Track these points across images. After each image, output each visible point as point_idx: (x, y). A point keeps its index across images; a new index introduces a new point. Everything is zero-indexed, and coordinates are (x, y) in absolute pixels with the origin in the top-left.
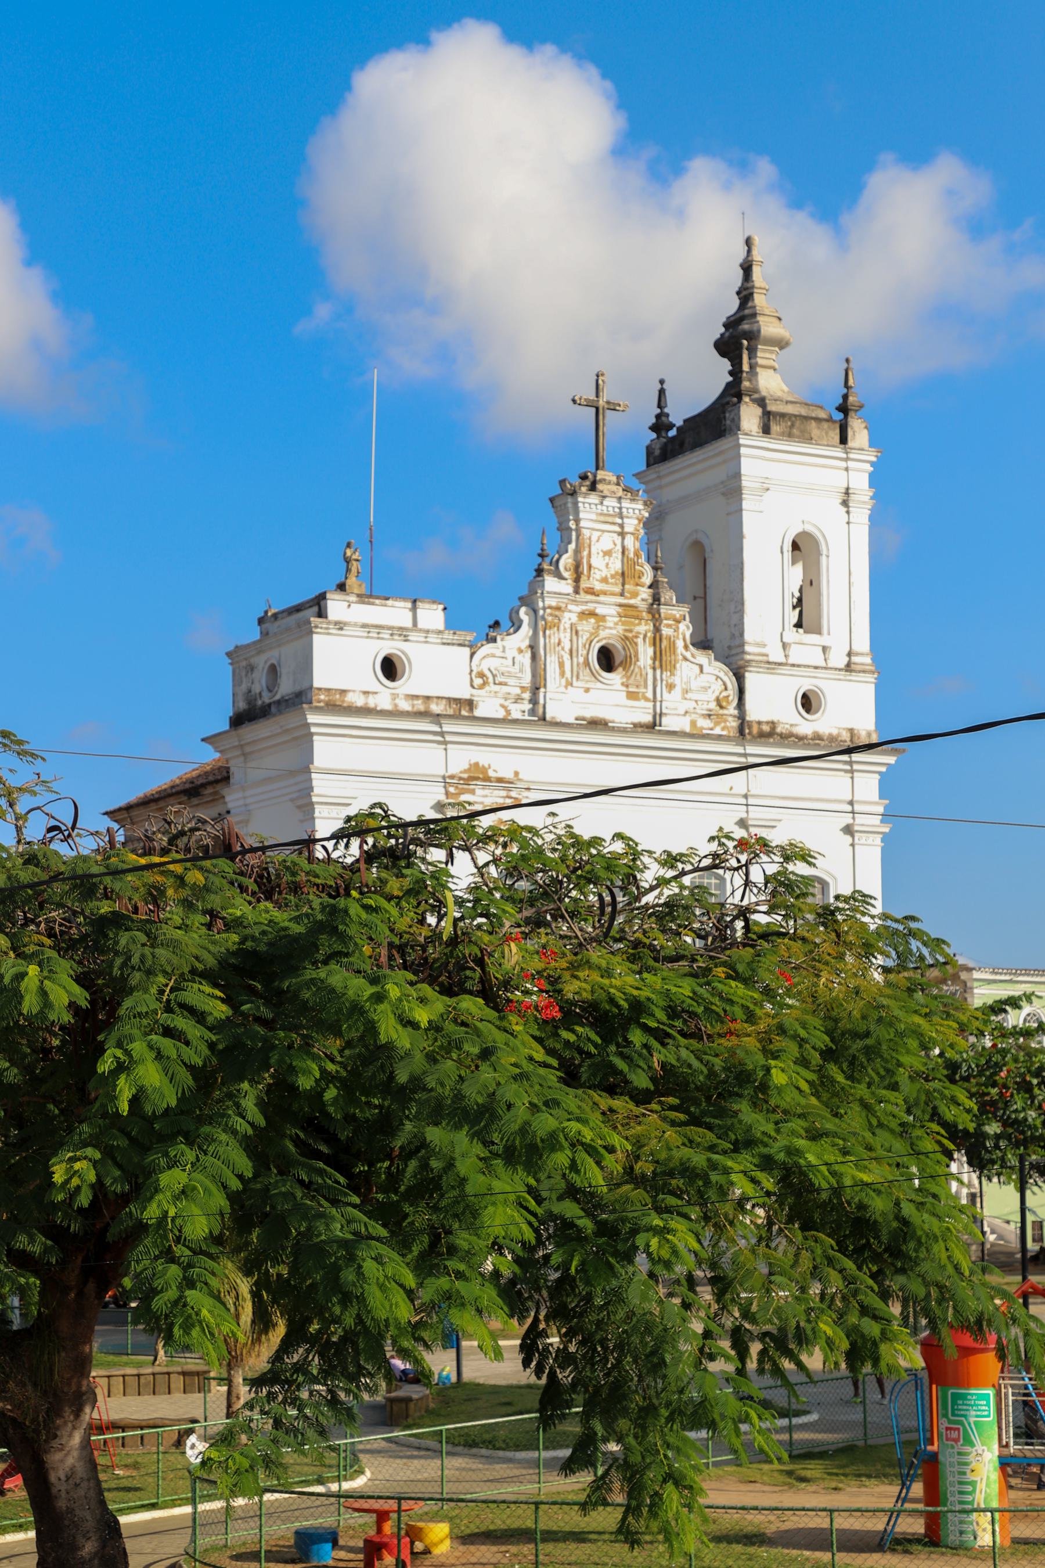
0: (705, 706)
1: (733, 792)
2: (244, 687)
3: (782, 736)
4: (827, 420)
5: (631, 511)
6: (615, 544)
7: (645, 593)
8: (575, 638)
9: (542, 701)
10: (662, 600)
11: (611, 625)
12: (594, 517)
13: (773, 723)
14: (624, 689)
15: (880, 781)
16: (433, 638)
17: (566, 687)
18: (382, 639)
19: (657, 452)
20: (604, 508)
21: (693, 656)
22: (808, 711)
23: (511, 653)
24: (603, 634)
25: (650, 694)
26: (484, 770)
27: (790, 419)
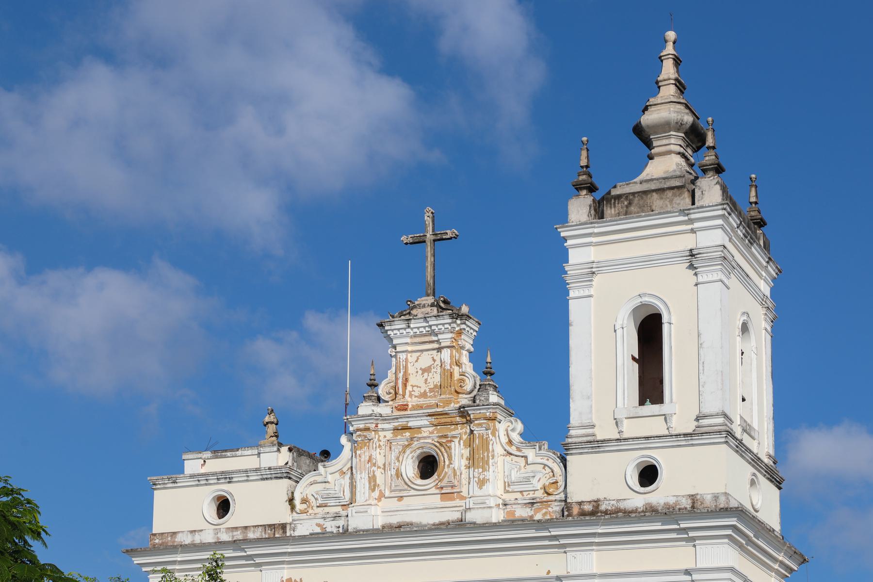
0: (531, 495)
3: (606, 512)
6: (434, 360)
12: (408, 340)
14: (437, 491)
21: (518, 449)
27: (627, 198)
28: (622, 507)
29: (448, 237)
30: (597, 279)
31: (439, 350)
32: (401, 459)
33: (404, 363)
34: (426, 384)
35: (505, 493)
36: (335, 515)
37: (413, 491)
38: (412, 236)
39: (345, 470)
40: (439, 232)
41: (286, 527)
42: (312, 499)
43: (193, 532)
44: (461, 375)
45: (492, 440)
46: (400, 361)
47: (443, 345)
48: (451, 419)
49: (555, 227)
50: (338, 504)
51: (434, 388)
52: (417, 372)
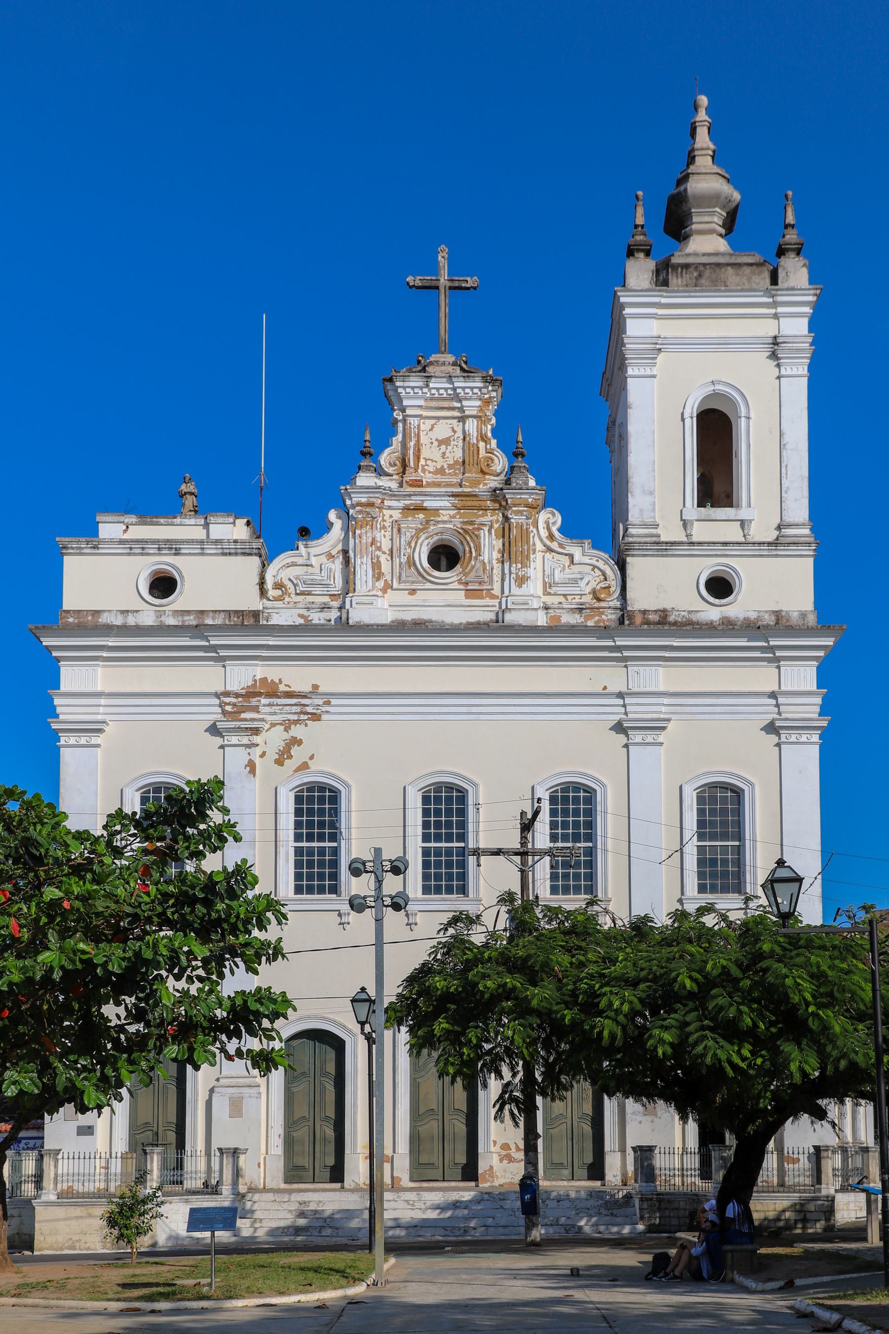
3: (675, 623)
6: (454, 432)
11: (446, 518)
12: (421, 402)
13: (664, 611)
14: (462, 587)
15: (818, 668)
20: (434, 391)
25: (497, 591)
29: (468, 286)
30: (661, 357)
31: (462, 419)
32: (413, 545)
33: (416, 430)
34: (443, 458)
35: (544, 595)
36: (323, 606)
37: (428, 584)
38: (422, 278)
39: (334, 552)
40: (456, 278)
41: (259, 615)
42: (289, 585)
44: (488, 453)
45: (532, 531)
46: (410, 428)
47: (467, 413)
48: (479, 502)
49: (616, 289)
50: (326, 593)
51: (454, 464)
52: (432, 443)
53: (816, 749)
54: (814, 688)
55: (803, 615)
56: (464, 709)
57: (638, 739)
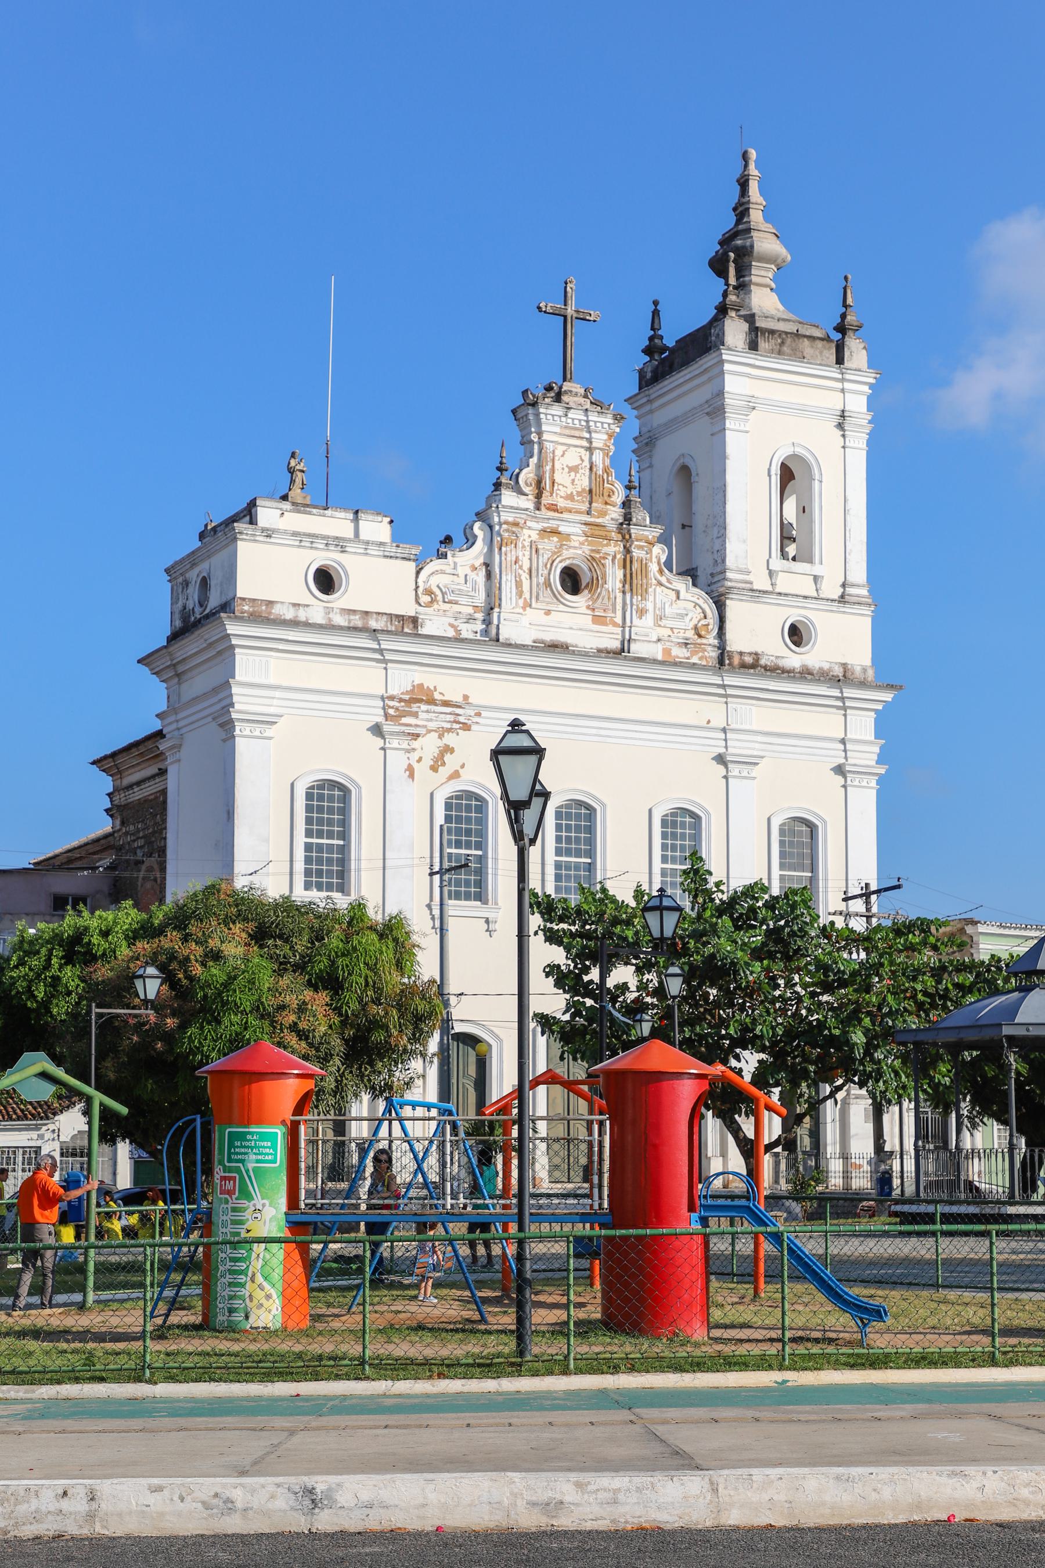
0: (681, 635)
1: (711, 725)
2: (180, 605)
3: (765, 668)
4: (822, 339)
5: (599, 425)
6: (582, 460)
7: (615, 513)
8: (534, 556)
9: (495, 622)
10: (634, 520)
11: (577, 544)
12: (557, 430)
13: (756, 654)
14: (589, 612)
16: (373, 551)
17: (524, 608)
18: (316, 548)
19: (649, 375)
20: (570, 421)
21: (669, 581)
22: (797, 644)
23: (461, 571)
24: (566, 553)
26: (429, 692)
28: (781, 665)
42: (438, 592)
43: (295, 605)
53: (873, 794)
54: (872, 738)
55: (864, 670)
56: (594, 731)
57: (736, 773)
